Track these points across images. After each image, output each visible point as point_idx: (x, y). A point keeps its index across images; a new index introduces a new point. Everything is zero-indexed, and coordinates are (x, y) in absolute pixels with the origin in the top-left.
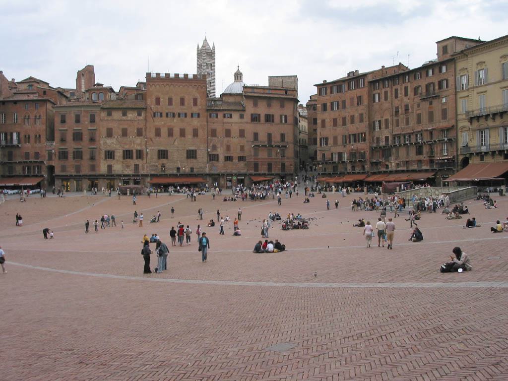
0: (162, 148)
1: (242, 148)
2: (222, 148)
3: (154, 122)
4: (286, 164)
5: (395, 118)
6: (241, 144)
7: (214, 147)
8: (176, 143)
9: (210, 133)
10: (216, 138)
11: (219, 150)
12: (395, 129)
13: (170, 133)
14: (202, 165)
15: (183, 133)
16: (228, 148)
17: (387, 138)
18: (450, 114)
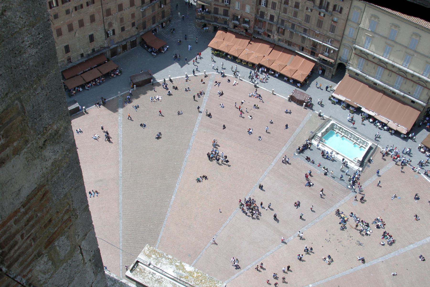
0: (65, 45)
1: (133, 16)
2: (117, 23)
3: (54, 24)
4: (166, 10)
5: (283, 6)
6: (133, 13)
7: (110, 25)
8: (77, 34)
9: (105, 14)
10: (111, 16)
11: (114, 25)
12: (283, 14)
13: (70, 28)
14: (102, 43)
15: (81, 24)
16: (122, 20)
17: (272, 17)
18: (338, 31)
